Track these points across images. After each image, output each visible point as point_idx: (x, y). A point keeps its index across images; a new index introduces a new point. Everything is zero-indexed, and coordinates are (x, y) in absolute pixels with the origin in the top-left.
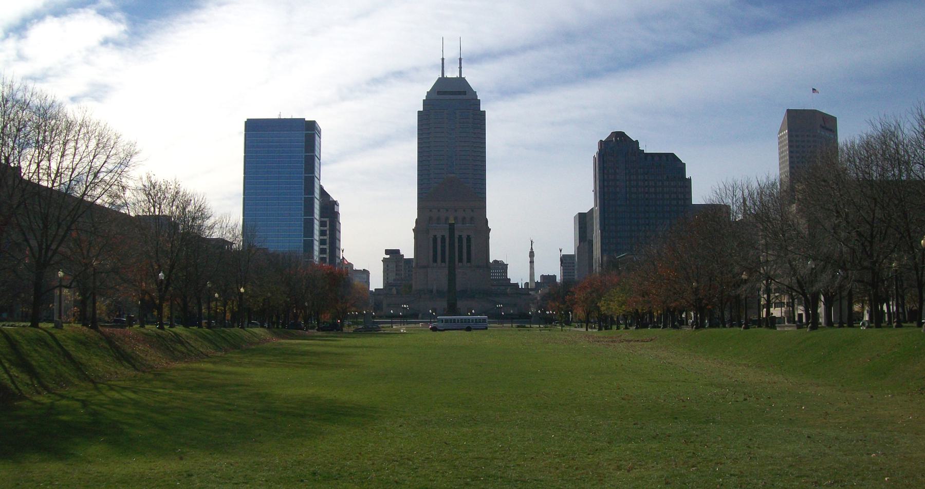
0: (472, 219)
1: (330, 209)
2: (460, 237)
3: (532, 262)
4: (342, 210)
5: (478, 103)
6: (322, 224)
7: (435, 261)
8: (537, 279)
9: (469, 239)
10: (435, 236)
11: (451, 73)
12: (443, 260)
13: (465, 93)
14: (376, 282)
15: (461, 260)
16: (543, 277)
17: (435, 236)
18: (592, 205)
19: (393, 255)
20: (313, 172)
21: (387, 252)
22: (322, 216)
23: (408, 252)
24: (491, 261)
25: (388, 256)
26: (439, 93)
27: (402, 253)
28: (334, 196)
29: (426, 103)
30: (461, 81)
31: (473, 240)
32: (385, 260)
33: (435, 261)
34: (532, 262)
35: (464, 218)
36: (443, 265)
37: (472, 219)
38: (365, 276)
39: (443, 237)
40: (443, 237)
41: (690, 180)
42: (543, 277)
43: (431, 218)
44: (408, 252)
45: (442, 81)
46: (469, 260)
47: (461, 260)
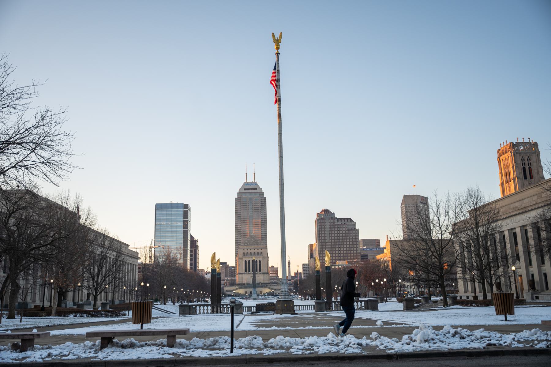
0: (261, 253)
1: (194, 243)
4: (199, 244)
6: (191, 251)
7: (246, 271)
9: (260, 261)
11: (250, 180)
12: (249, 271)
13: (256, 189)
16: (295, 273)
22: (191, 247)
24: (270, 266)
26: (245, 189)
28: (196, 238)
30: (255, 183)
31: (261, 262)
37: (261, 253)
39: (249, 261)
43: (244, 253)
45: (246, 184)
46: (260, 271)
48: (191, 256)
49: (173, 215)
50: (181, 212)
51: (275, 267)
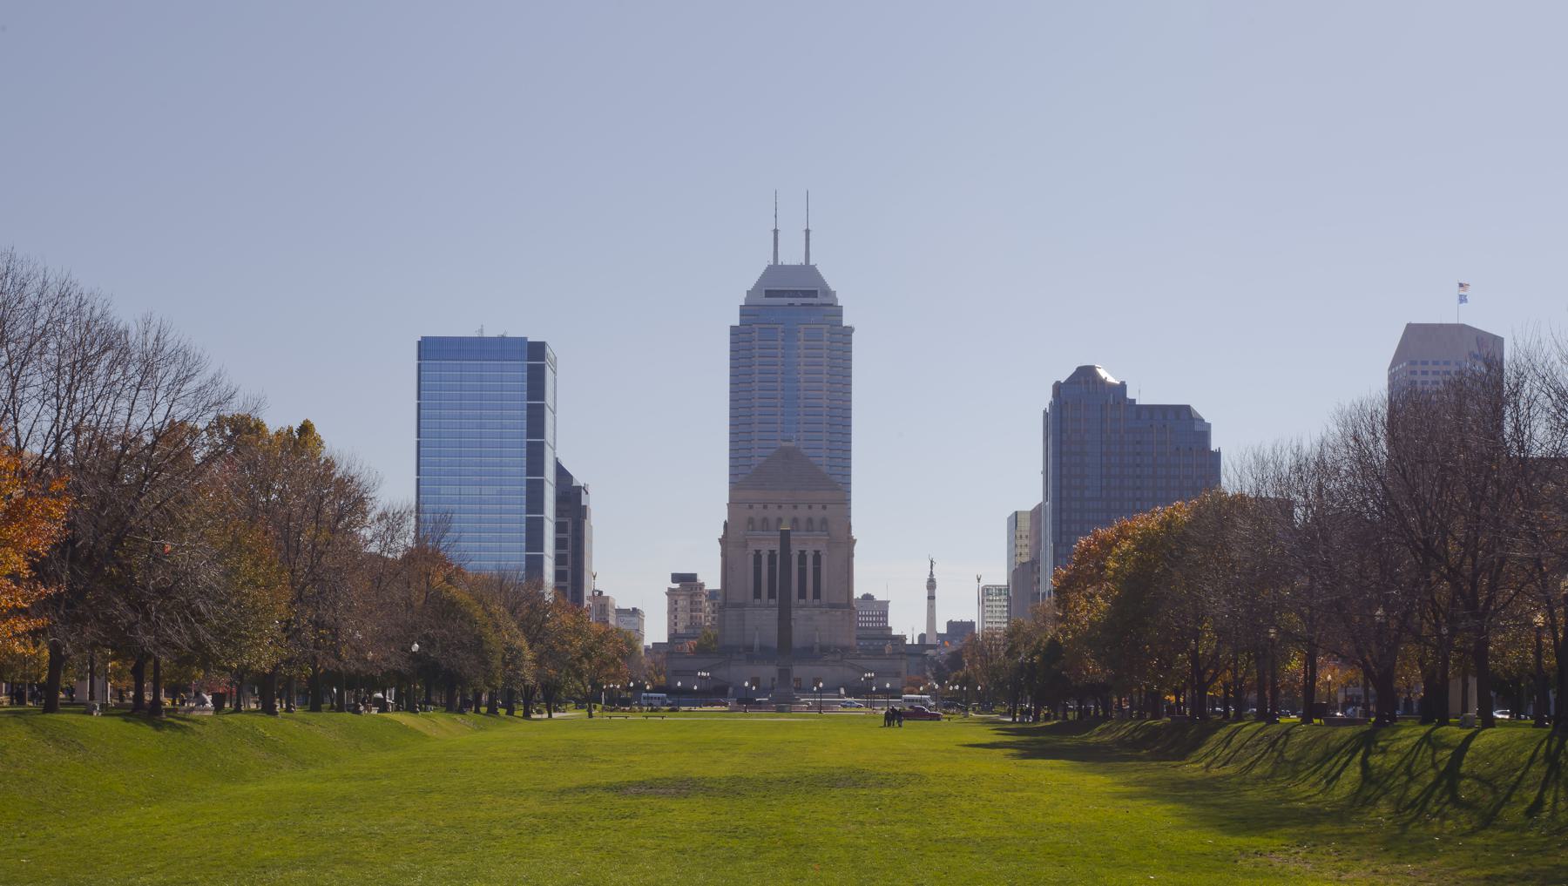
0: (824, 521)
1: (572, 501)
2: (802, 554)
3: (931, 598)
5: (838, 312)
6: (560, 528)
7: (757, 594)
8: (942, 629)
9: (817, 557)
10: (758, 552)
11: (791, 256)
12: (771, 595)
13: (813, 294)
14: (655, 631)
15: (802, 595)
16: (951, 624)
17: (758, 552)
18: (1040, 500)
19: (686, 582)
20: (542, 435)
21: (676, 578)
22: (559, 512)
23: (711, 579)
24: (858, 593)
25: (677, 586)
26: (769, 294)
27: (700, 579)
28: (579, 479)
29: (745, 311)
30: (808, 270)
32: (671, 593)
33: (757, 594)
34: (931, 598)
35: (810, 521)
36: (772, 602)
37: (824, 521)
38: (635, 620)
40: (772, 552)
41: (1217, 455)
42: (951, 624)
44: (711, 579)
45: (774, 270)
46: (817, 595)
47: (802, 595)
48: (560, 543)
49: (490, 386)
50: (517, 373)
51: (878, 597)
